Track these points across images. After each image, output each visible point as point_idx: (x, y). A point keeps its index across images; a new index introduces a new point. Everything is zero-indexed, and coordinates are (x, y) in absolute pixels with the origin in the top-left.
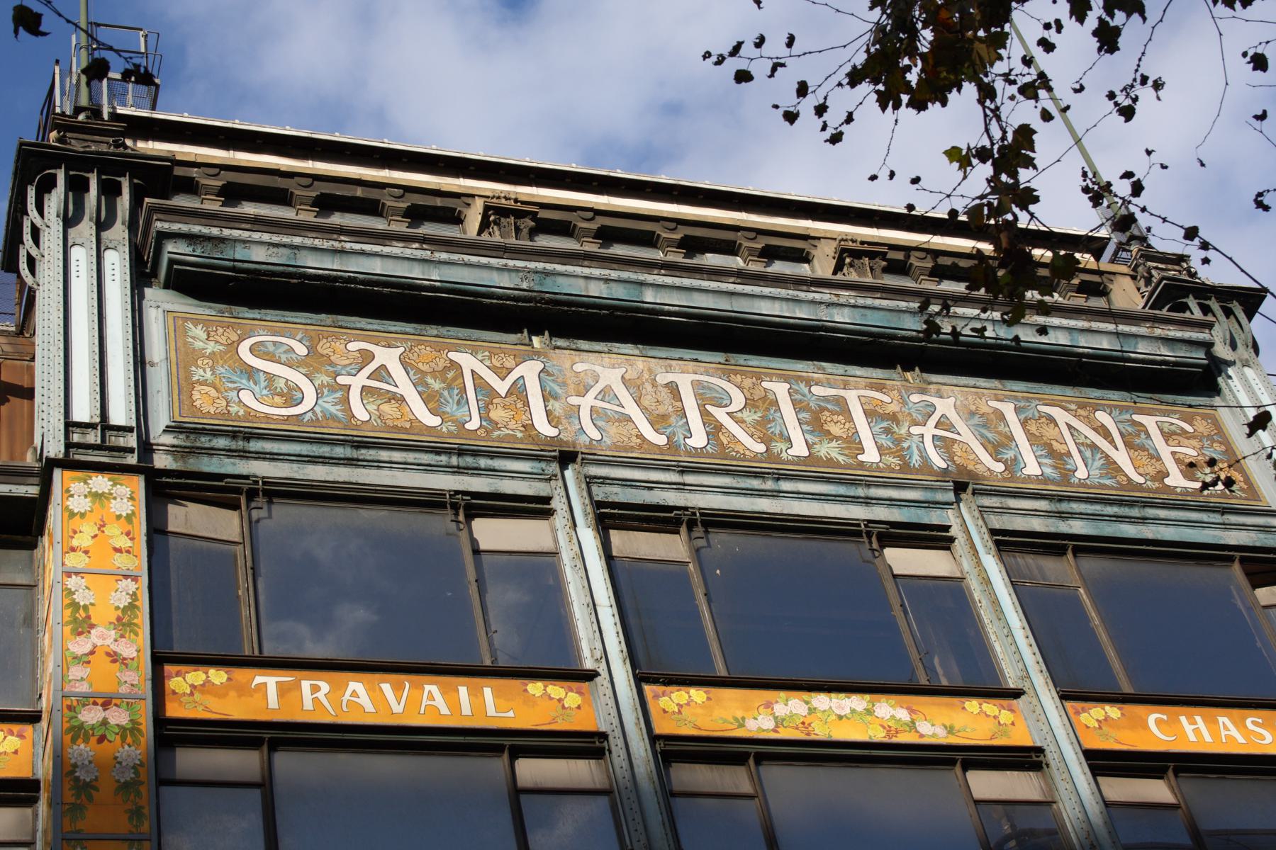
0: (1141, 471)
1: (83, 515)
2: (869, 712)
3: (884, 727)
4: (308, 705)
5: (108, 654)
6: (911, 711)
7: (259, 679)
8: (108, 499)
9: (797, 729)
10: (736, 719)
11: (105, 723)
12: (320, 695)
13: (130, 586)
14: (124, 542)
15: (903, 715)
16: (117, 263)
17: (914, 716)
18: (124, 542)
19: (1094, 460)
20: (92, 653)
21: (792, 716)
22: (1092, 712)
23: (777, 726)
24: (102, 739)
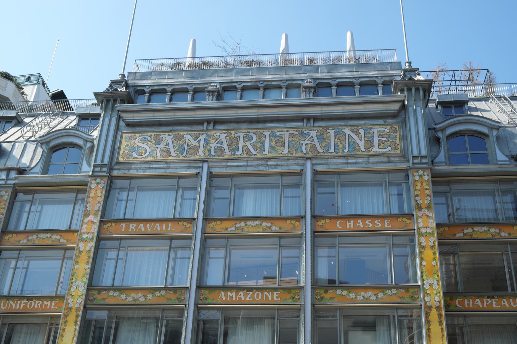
0: (366, 147)
1: (93, 188)
2: (260, 224)
3: (263, 228)
4: (130, 230)
5: (91, 222)
6: (272, 223)
7: (122, 224)
8: (99, 184)
9: (240, 230)
10: (226, 228)
11: (87, 237)
12: (133, 227)
13: (99, 205)
14: (100, 194)
15: (269, 225)
16: (114, 120)
17: (272, 225)
18: (100, 194)
19: (352, 145)
20: (88, 221)
21: (241, 226)
22: (322, 221)
23: (235, 229)
24: (86, 241)
